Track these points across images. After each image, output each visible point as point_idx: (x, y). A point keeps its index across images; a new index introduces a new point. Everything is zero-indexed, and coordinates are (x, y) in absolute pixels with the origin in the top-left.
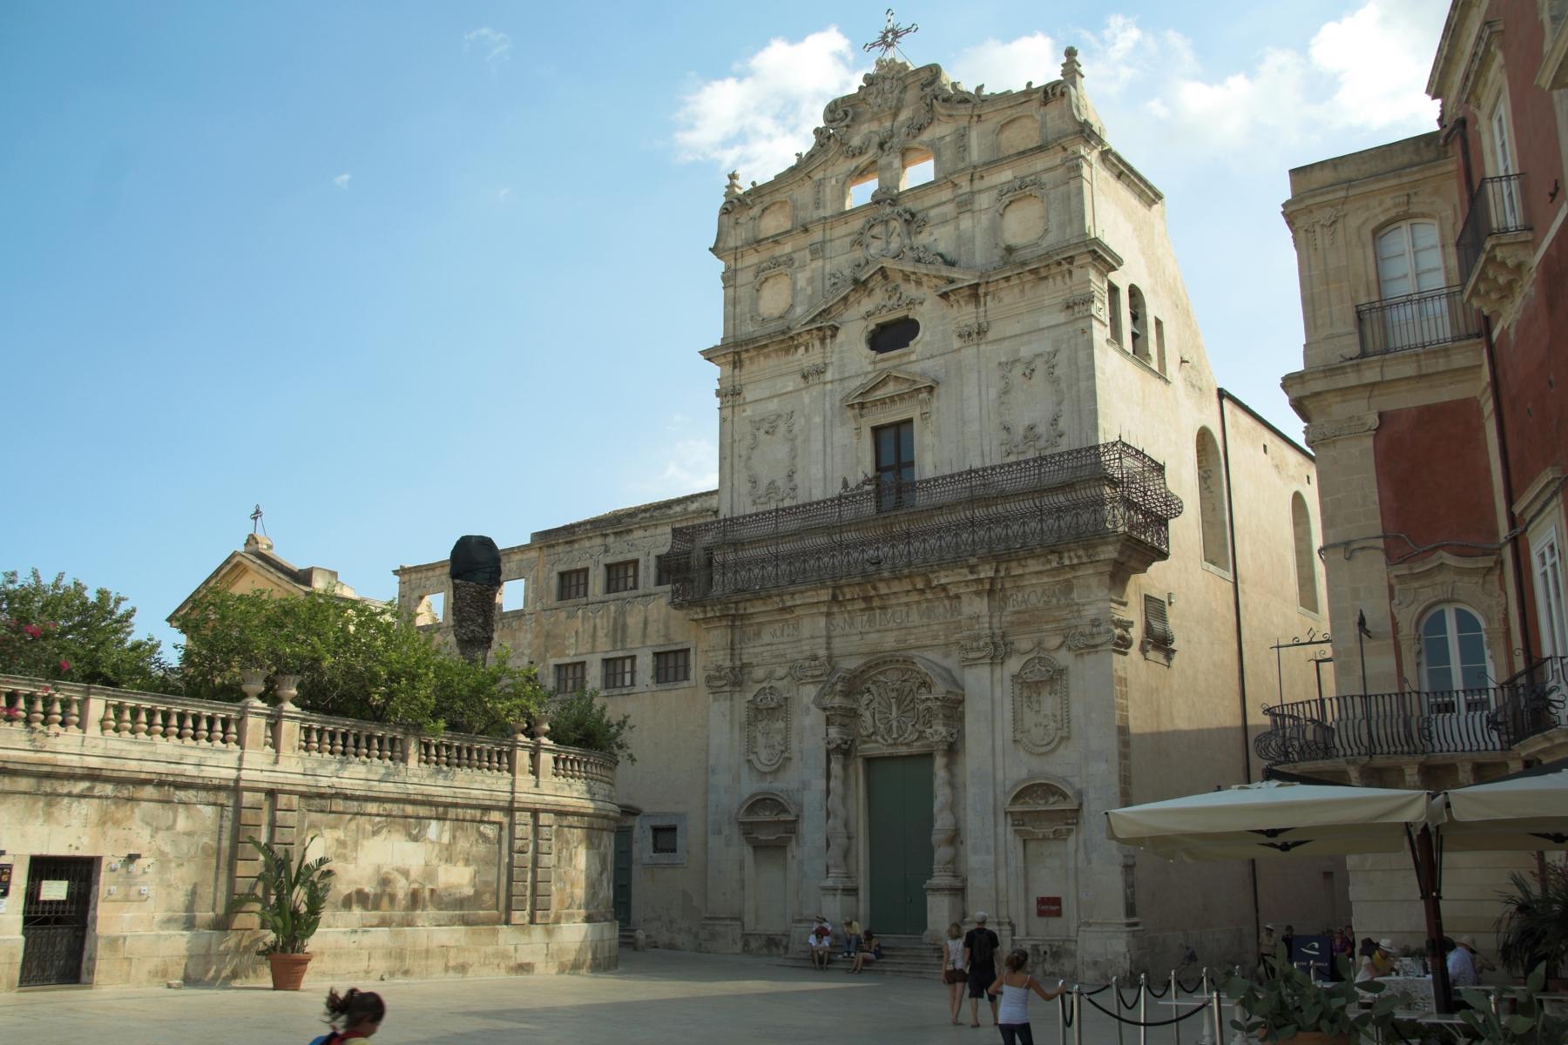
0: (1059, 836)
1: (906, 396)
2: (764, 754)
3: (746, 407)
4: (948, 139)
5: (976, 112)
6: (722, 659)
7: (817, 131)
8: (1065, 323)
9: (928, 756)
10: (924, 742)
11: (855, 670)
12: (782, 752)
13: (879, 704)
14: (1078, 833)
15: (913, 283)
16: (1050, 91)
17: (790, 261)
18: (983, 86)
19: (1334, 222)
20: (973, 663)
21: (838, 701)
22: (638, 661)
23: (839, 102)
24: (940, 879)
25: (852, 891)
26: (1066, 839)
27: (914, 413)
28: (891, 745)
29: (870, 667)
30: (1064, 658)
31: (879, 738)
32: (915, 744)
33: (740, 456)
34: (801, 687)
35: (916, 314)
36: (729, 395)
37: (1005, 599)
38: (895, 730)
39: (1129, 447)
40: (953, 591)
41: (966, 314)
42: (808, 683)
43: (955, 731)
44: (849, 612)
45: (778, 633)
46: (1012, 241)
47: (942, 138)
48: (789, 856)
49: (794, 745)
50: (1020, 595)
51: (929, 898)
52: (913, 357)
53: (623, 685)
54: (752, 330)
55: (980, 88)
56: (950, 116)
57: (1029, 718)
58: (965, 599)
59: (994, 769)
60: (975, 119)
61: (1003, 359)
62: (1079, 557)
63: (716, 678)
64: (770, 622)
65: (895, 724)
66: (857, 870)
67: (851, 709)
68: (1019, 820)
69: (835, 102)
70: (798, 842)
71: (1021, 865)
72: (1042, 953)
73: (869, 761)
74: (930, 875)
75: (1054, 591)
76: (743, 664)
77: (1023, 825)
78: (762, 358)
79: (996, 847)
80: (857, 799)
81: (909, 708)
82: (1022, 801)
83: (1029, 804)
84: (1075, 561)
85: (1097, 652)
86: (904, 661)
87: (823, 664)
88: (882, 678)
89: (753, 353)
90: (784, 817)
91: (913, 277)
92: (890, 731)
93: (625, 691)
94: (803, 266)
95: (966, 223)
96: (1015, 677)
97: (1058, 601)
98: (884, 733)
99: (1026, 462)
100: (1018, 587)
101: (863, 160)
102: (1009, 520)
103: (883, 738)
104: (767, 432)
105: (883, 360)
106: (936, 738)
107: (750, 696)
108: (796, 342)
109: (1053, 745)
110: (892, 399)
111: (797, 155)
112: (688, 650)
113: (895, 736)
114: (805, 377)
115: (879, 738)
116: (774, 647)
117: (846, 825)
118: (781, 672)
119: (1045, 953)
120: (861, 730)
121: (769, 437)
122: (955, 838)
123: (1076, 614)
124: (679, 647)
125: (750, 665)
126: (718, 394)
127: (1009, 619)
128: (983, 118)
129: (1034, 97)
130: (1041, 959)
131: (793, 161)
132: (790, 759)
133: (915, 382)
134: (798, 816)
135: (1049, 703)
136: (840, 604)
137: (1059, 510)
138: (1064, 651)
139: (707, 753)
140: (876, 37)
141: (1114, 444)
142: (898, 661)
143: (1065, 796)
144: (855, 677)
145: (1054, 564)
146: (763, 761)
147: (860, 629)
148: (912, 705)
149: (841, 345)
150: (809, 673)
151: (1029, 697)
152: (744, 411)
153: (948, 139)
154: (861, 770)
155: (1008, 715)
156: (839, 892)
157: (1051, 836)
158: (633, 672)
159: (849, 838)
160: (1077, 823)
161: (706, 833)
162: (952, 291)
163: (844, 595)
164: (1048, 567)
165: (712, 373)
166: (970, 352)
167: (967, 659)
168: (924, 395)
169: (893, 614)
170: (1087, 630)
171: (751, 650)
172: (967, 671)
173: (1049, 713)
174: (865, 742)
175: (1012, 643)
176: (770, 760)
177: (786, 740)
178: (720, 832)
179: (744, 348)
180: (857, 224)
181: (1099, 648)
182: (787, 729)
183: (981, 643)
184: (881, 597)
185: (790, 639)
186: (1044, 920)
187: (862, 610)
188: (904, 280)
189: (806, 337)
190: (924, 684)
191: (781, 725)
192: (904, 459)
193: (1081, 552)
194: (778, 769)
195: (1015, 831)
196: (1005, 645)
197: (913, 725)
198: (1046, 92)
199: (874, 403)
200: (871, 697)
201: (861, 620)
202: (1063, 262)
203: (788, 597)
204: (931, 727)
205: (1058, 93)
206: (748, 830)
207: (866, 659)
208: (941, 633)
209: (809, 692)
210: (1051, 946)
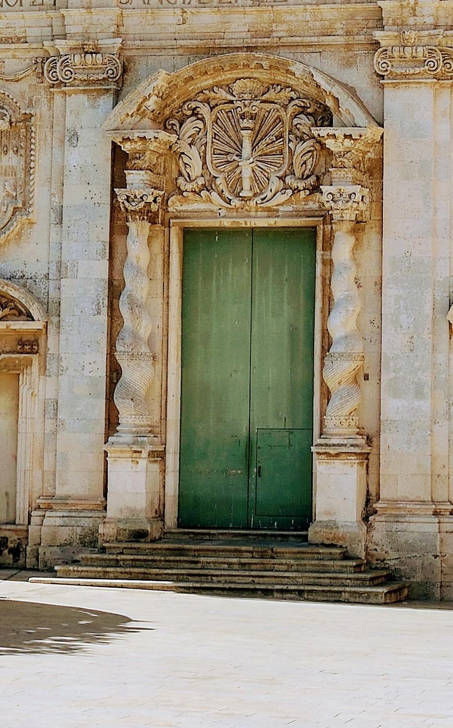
31: (214, 195)
32: (281, 208)
48: (24, 390)
65: (247, 174)
70: (44, 369)
73: (188, 234)
86: (271, 67)
103: (221, 194)
120: (181, 181)
182: (28, 170)
200: (201, 125)
208: (338, 25)
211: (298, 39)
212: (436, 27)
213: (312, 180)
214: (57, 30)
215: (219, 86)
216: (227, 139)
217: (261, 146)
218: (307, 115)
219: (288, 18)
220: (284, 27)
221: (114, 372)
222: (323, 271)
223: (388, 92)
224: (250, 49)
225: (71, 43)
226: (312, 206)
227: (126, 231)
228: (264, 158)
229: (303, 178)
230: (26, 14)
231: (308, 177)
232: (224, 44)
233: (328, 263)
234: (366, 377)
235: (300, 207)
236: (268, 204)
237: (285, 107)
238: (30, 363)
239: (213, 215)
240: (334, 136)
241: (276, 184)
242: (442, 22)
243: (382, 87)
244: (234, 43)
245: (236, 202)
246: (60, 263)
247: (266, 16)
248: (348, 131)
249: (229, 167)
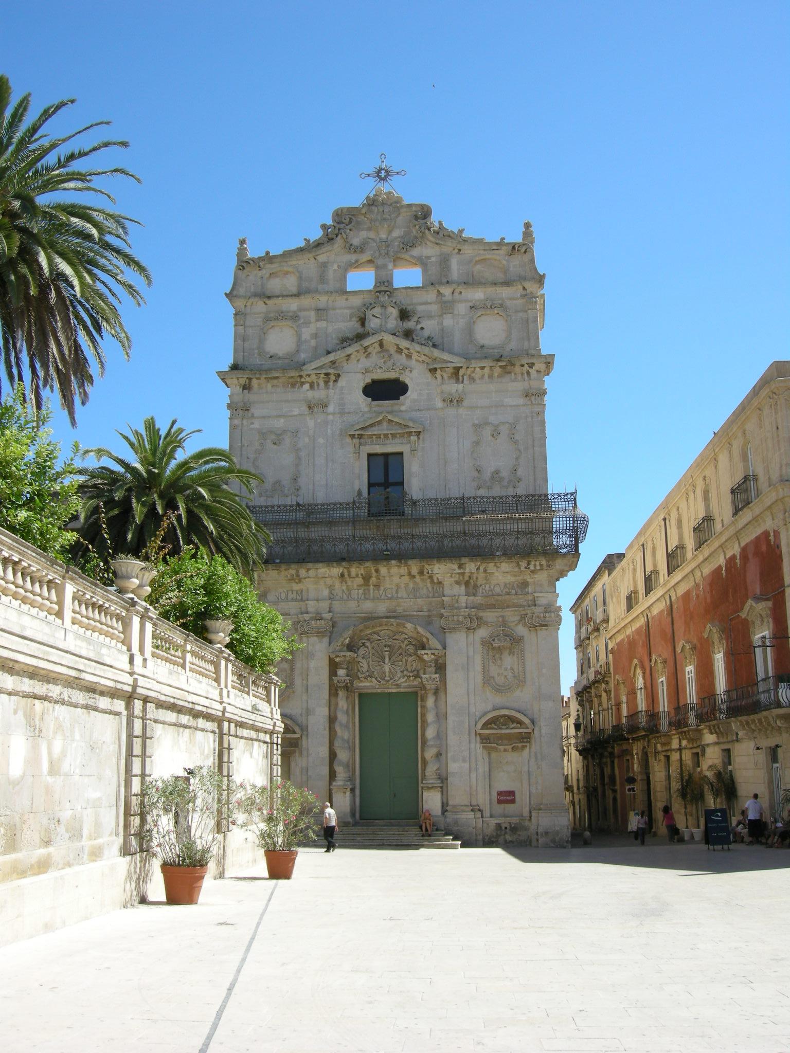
1: (398, 436)
3: (253, 420)
4: (433, 259)
5: (459, 247)
7: (324, 227)
8: (524, 405)
13: (373, 654)
14: (530, 748)
17: (295, 317)
18: (464, 230)
20: (453, 630)
23: (345, 211)
27: (404, 448)
30: (521, 630)
32: (403, 685)
33: (248, 458)
35: (406, 379)
36: (238, 409)
37: (475, 587)
38: (387, 674)
41: (453, 388)
45: (283, 596)
46: (482, 342)
47: (428, 258)
48: (293, 764)
50: (487, 586)
52: (403, 408)
54: (259, 363)
55: (461, 231)
56: (437, 244)
57: (494, 670)
59: (469, 704)
60: (456, 251)
61: (476, 422)
65: (387, 670)
68: (485, 740)
69: (342, 209)
70: (301, 754)
71: (487, 769)
73: (361, 696)
75: (513, 586)
77: (489, 743)
78: (269, 386)
79: (470, 758)
86: (397, 625)
89: (263, 380)
91: (406, 351)
94: (307, 323)
95: (448, 321)
96: (484, 643)
101: (365, 257)
103: (376, 679)
104: (275, 444)
105: (379, 406)
108: (303, 380)
110: (386, 436)
111: (305, 239)
114: (310, 407)
119: (506, 828)
121: (275, 447)
126: (229, 406)
128: (461, 252)
129: (504, 248)
130: (503, 833)
131: (302, 244)
133: (407, 427)
135: (509, 661)
140: (371, 170)
143: (520, 722)
149: (342, 388)
152: (252, 423)
153: (433, 259)
155: (478, 667)
157: (510, 750)
160: (529, 742)
162: (441, 368)
165: (223, 394)
166: (451, 411)
168: (414, 438)
173: (509, 667)
174: (361, 681)
175: (481, 618)
179: (258, 376)
180: (357, 301)
186: (502, 806)
189: (313, 378)
192: (391, 480)
193: (544, 562)
195: (483, 747)
196: (477, 619)
198: (514, 248)
199: (371, 436)
200: (366, 649)
202: (526, 365)
205: (523, 250)
208: (425, 607)
210: (510, 823)
211: (408, 613)
212: (466, 608)
213: (415, 673)
214: (303, 610)
215: (374, 633)
216: (378, 656)
218: (413, 645)
219: (403, 604)
220: (401, 608)
221: (333, 756)
222: (421, 710)
223: (447, 635)
224: (387, 617)
225: (311, 615)
226: (416, 683)
227: (336, 695)
228: (394, 663)
229: (411, 672)
230: (290, 603)
231: (414, 671)
232: (376, 615)
233: (423, 707)
234: (441, 754)
235: (411, 683)
236: (397, 683)
237: (403, 642)
239: (374, 688)
240: (427, 654)
241: (399, 674)
242: (469, 605)
243: (445, 632)
244: (382, 615)
245: (383, 682)
246: (307, 709)
247: (394, 603)
248: (433, 652)
249: (379, 667)
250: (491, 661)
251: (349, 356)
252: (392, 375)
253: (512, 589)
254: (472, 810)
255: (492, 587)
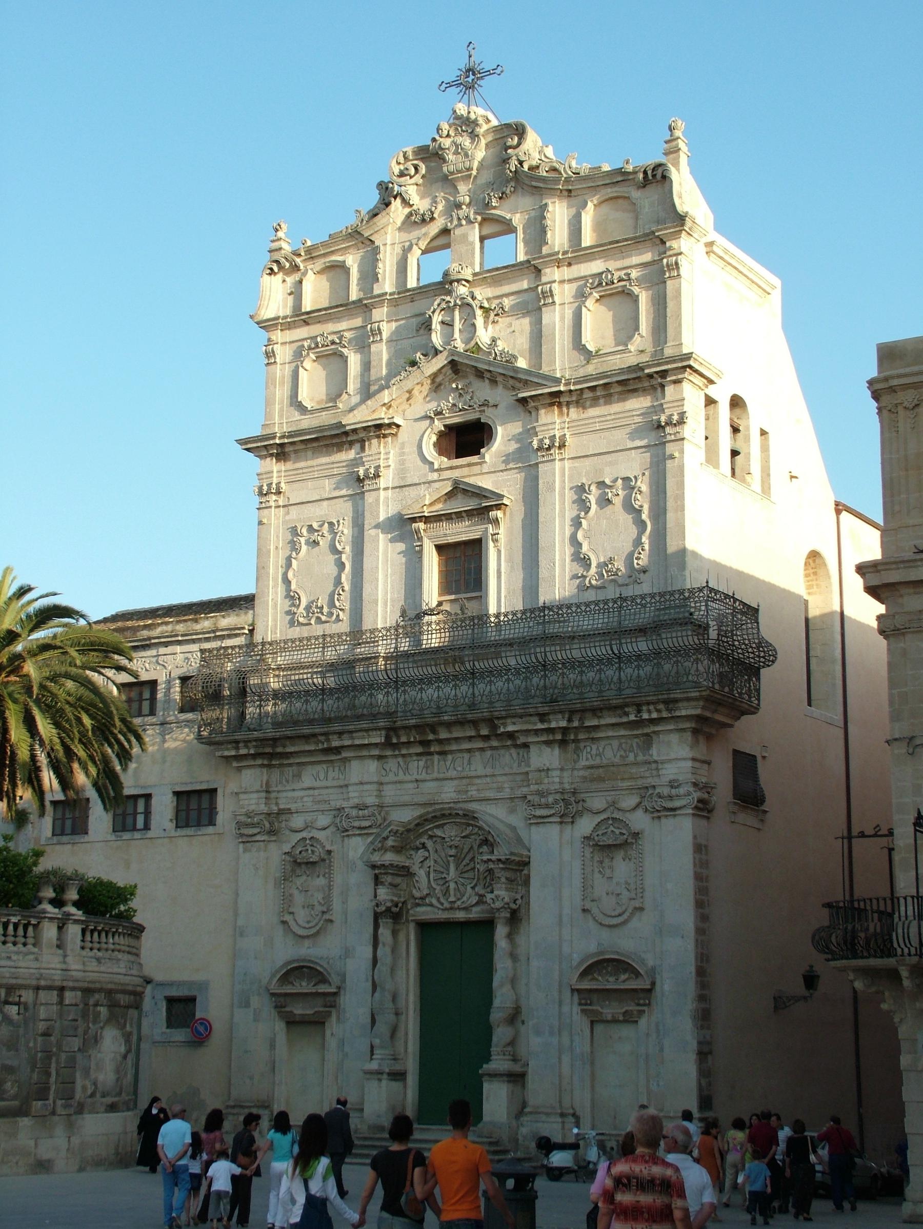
0: (629, 1019)
2: (302, 915)
6: (254, 803)
9: (487, 925)
10: (484, 907)
11: (409, 822)
12: (323, 912)
13: (435, 861)
15: (487, 381)
16: (649, 173)
19: (917, 405)
20: (541, 821)
21: (389, 857)
22: (154, 801)
24: (498, 1063)
25: (398, 1076)
26: (637, 1022)
28: (446, 909)
29: (426, 820)
30: (639, 821)
31: (434, 901)
34: (346, 839)
39: (717, 592)
40: (522, 740)
42: (354, 835)
43: (518, 896)
44: (403, 756)
45: (322, 776)
48: (328, 1033)
49: (337, 905)
50: (595, 747)
51: (486, 1086)
53: (134, 829)
57: (600, 886)
58: (533, 748)
62: (658, 711)
63: (248, 825)
64: (313, 763)
65: (452, 886)
66: (406, 1051)
67: (403, 867)
68: (585, 997)
71: (587, 1048)
72: (608, 1149)
73: (424, 927)
74: (487, 1058)
75: (632, 746)
76: (279, 810)
77: (590, 1005)
80: (408, 970)
81: (469, 867)
82: (590, 977)
83: (597, 980)
84: (655, 715)
85: (675, 816)
87: (373, 815)
88: (439, 832)
90: (323, 988)
91: (487, 375)
92: (446, 893)
93: (137, 835)
97: (635, 757)
98: (440, 895)
99: (606, 602)
100: (593, 739)
102: (585, 666)
103: (438, 899)
106: (498, 904)
107: (287, 848)
109: (625, 916)
112: (215, 790)
113: (452, 899)
115: (434, 901)
116: (316, 792)
117: (394, 998)
118: (323, 820)
120: (414, 891)
122: (515, 1017)
123: (655, 773)
124: (204, 787)
125: (289, 811)
127: (581, 773)
128: (573, 194)
132: (331, 921)
134: (339, 988)
135: (622, 868)
136: (395, 746)
137: (639, 657)
138: (640, 813)
139: (236, 915)
141: (701, 590)
142: (457, 814)
143: (637, 974)
144: (409, 831)
145: (632, 717)
146: (301, 922)
147: (416, 776)
148: (472, 865)
150: (357, 824)
151: (601, 862)
154: (412, 937)
155: (577, 882)
156: (385, 1076)
157: (621, 1018)
158: (147, 813)
159: (397, 1014)
160: (649, 1004)
161: (232, 1006)
162: (531, 397)
163: (398, 737)
164: (625, 720)
167: (534, 816)
169: (453, 760)
170: (666, 791)
171: (290, 794)
172: (533, 828)
174: (418, 905)
176: (308, 922)
177: (328, 899)
178: (247, 1005)
181: (678, 812)
182: (330, 887)
183: (551, 799)
184: (440, 742)
185: (335, 783)
187: (418, 754)
188: (477, 376)
190: (485, 842)
191: (321, 881)
193: (661, 706)
194: (318, 932)
195: (582, 1011)
197: (473, 888)
200: (426, 854)
201: (416, 766)
202: (655, 375)
203: (335, 737)
204: (492, 892)
206: (280, 1002)
207: (419, 812)
208: (506, 785)
209: (357, 847)
217: (461, 867)
238: (329, 1014)
250: (596, 870)
251: (410, 392)
252: (471, 416)
253: (630, 751)
254: (562, 1115)
255: (601, 750)
